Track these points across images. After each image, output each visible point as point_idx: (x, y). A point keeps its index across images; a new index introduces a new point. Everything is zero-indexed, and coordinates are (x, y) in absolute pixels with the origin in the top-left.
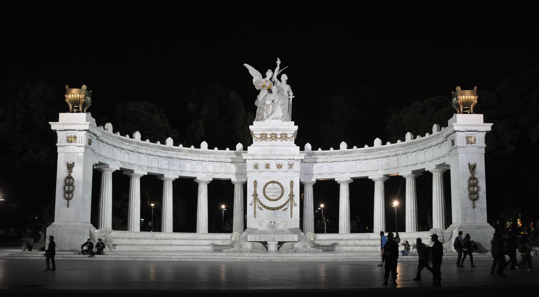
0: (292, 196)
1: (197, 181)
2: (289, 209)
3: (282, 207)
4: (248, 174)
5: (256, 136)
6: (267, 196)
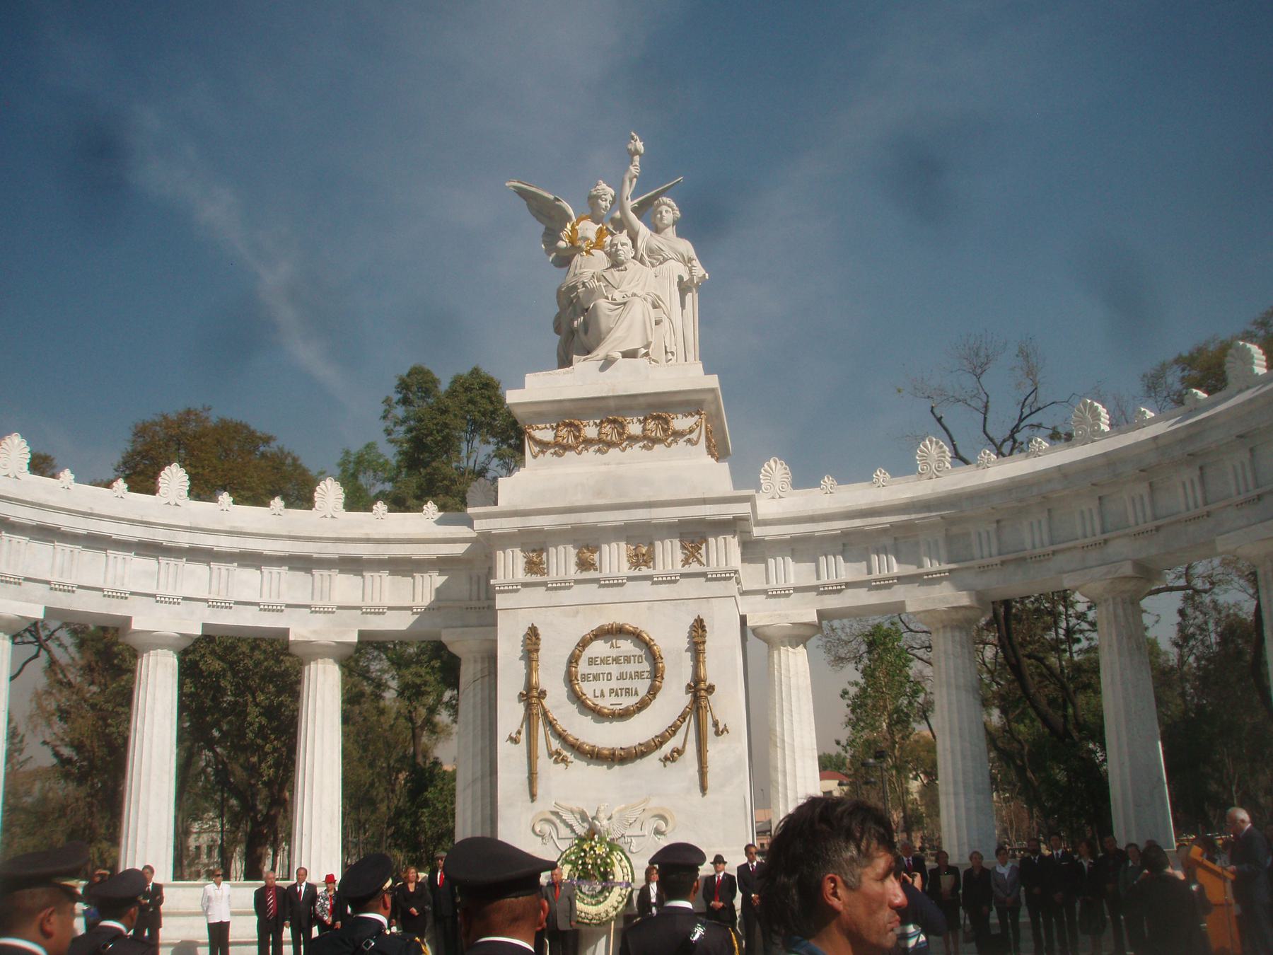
0: (699, 690)
2: (691, 749)
4: (501, 601)
5: (538, 435)
6: (590, 695)
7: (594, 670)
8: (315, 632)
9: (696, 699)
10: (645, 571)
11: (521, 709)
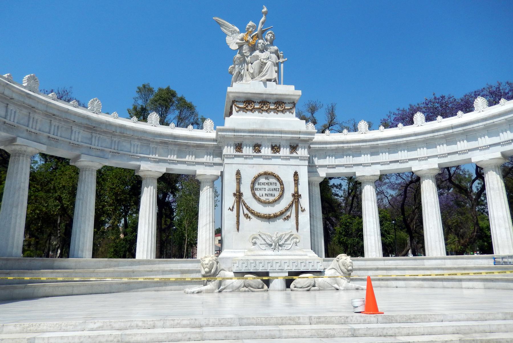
0: (297, 196)
1: (141, 174)
2: (293, 216)
3: (282, 213)
7: (260, 187)
8: (150, 167)
9: (295, 199)
10: (277, 154)
11: (233, 199)
